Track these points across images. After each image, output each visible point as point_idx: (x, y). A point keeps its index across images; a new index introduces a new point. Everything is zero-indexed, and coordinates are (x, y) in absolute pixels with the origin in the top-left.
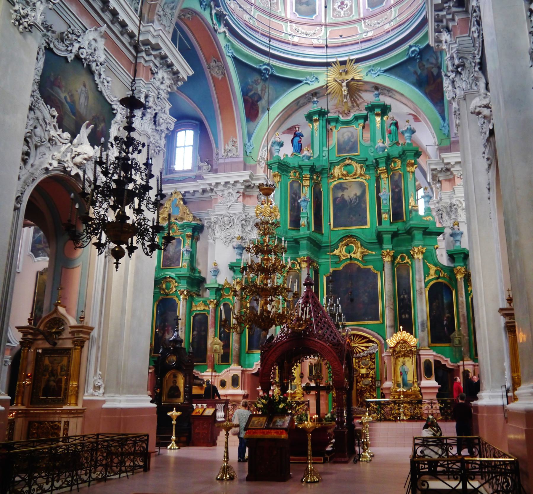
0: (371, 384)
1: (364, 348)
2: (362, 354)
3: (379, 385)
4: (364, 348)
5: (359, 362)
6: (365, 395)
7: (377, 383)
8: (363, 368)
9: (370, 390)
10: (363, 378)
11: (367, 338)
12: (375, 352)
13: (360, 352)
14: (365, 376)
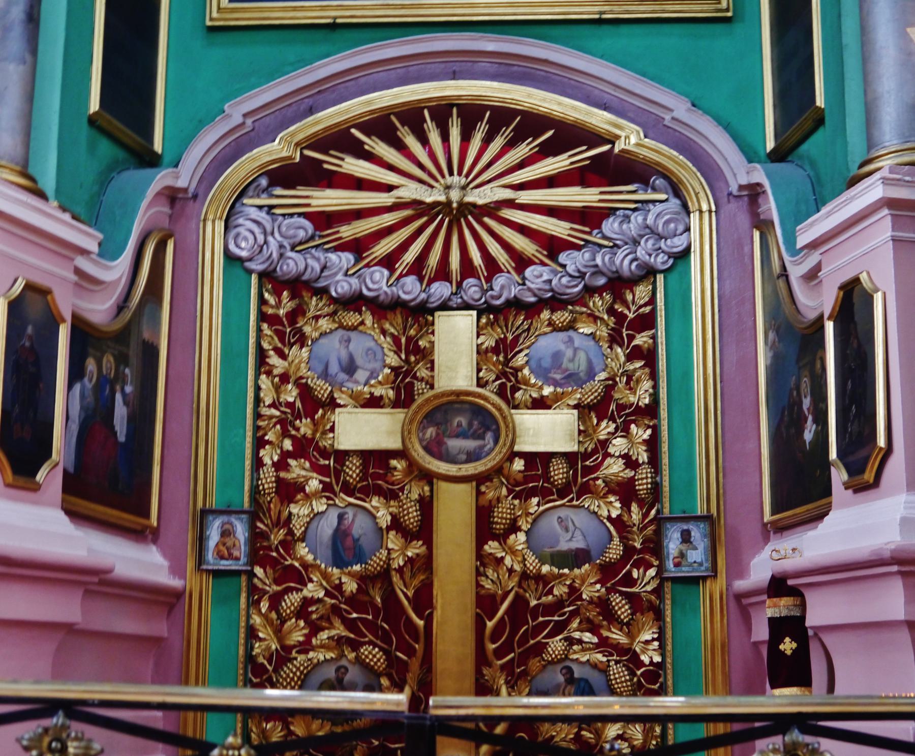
0: (615, 551)
1: (559, 228)
2: (538, 277)
3: (697, 555)
4: (559, 228)
5: (505, 348)
6: (556, 645)
7: (673, 545)
8: (540, 404)
9: (603, 605)
10: (544, 494)
11: (592, 138)
12: (660, 261)
13: (521, 262)
14: (559, 472)
